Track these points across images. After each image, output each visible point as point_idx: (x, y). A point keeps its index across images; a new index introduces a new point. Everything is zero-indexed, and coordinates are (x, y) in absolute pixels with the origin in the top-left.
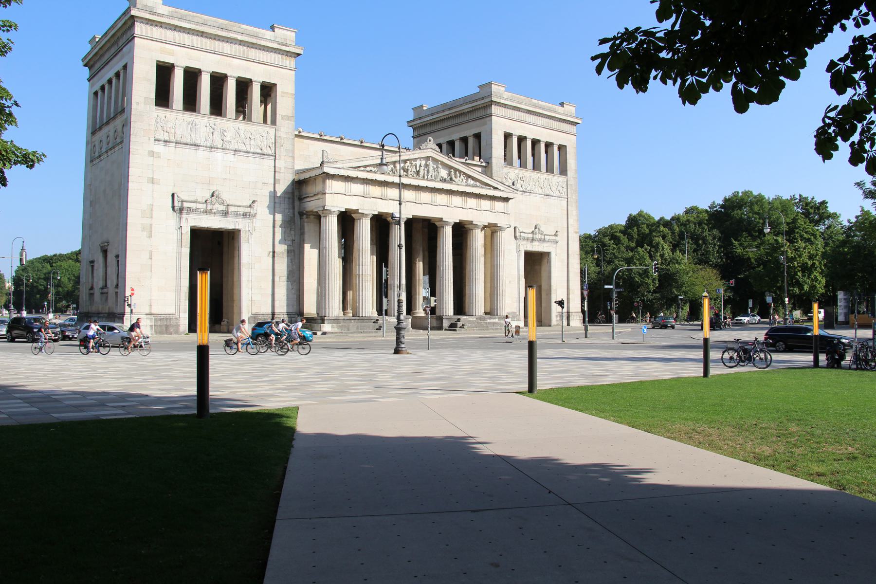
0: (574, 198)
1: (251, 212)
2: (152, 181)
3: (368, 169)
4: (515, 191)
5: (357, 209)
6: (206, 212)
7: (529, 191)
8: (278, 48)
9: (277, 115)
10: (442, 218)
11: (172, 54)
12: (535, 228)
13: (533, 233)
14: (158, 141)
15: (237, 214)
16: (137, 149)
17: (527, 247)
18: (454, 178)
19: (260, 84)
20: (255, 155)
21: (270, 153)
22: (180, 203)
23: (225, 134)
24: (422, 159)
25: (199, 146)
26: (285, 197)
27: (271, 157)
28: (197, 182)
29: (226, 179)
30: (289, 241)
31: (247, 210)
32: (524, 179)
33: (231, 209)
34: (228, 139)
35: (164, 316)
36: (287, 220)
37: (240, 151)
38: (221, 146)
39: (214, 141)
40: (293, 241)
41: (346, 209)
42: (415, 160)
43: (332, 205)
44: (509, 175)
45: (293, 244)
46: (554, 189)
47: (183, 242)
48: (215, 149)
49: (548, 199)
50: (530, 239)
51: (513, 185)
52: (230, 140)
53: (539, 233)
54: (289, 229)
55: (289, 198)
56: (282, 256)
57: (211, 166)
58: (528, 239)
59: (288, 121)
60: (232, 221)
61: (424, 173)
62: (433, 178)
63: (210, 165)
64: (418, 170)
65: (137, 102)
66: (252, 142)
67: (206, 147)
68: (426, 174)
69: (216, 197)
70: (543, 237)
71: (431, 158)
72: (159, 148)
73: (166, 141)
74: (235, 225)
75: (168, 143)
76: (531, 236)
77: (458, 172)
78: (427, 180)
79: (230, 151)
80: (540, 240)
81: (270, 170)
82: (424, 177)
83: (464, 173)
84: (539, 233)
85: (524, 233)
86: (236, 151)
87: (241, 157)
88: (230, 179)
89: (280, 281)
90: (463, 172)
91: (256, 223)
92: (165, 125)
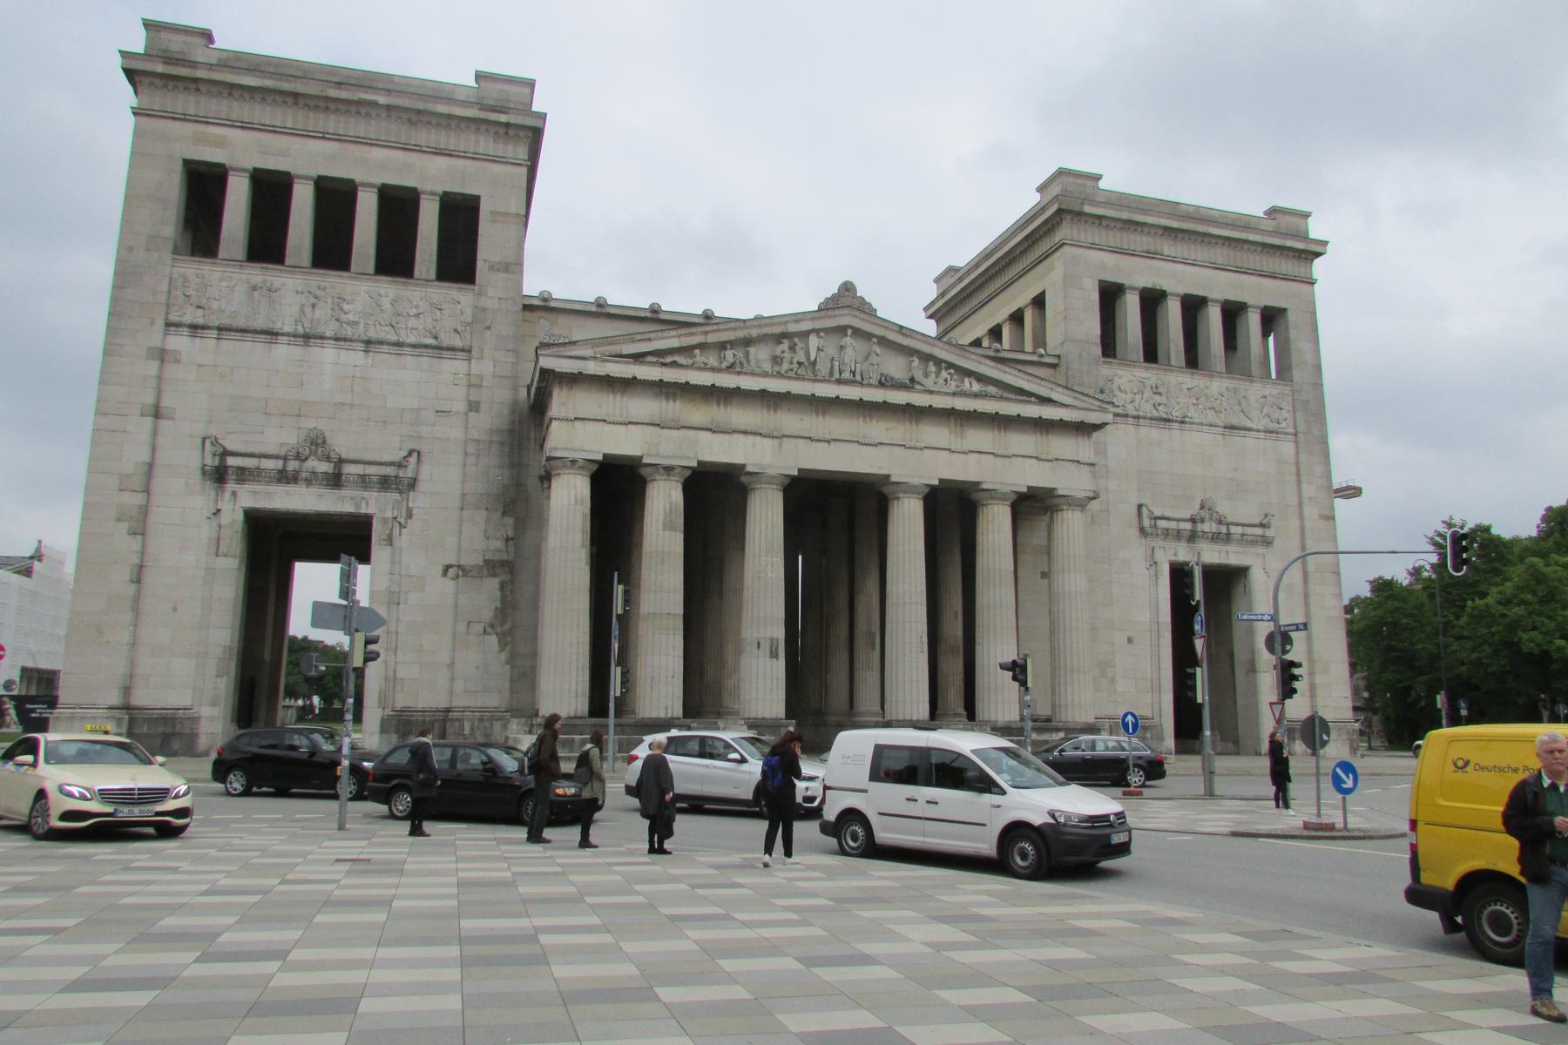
0: (1315, 432)
1: (401, 475)
2: (157, 413)
3: (669, 359)
4: (1104, 405)
5: (640, 454)
6: (285, 477)
7: (1180, 419)
8: (481, 117)
9: (480, 264)
10: (889, 476)
11: (221, 143)
12: (1202, 507)
13: (1193, 520)
14: (177, 325)
15: (364, 481)
16: (121, 346)
17: (1175, 554)
18: (919, 376)
19: (438, 198)
20: (421, 350)
21: (458, 343)
22: (217, 458)
23: (346, 307)
24: (822, 334)
26: (491, 442)
28: (268, 411)
29: (343, 404)
30: (497, 539)
31: (390, 471)
32: (1160, 390)
33: (349, 469)
34: (351, 317)
35: (160, 714)
36: (496, 492)
37: (381, 343)
38: (333, 333)
39: (314, 323)
40: (507, 540)
41: (605, 455)
42: (805, 335)
43: (569, 447)
44: (1117, 381)
45: (507, 547)
46: (1254, 414)
47: (221, 544)
49: (1237, 440)
50: (1186, 533)
51: (1102, 392)
52: (356, 320)
53: (1211, 519)
54: (499, 514)
55: (502, 444)
56: (476, 574)
57: (304, 378)
58: (1178, 535)
59: (505, 275)
60: (352, 498)
61: (832, 367)
62: (858, 378)
63: (302, 374)
64: (812, 359)
65: (129, 247)
66: (412, 323)
67: (295, 336)
68: (836, 369)
69: (311, 444)
70: (1224, 529)
71: (849, 332)
72: (179, 342)
73: (195, 328)
74: (358, 505)
76: (1188, 526)
77: (931, 364)
78: (839, 382)
80: (1215, 538)
82: (831, 374)
83: (950, 365)
84: (1211, 519)
85: (1168, 519)
86: (368, 342)
87: (383, 357)
88: (352, 405)
89: (468, 633)
90: (946, 362)
91: (414, 501)
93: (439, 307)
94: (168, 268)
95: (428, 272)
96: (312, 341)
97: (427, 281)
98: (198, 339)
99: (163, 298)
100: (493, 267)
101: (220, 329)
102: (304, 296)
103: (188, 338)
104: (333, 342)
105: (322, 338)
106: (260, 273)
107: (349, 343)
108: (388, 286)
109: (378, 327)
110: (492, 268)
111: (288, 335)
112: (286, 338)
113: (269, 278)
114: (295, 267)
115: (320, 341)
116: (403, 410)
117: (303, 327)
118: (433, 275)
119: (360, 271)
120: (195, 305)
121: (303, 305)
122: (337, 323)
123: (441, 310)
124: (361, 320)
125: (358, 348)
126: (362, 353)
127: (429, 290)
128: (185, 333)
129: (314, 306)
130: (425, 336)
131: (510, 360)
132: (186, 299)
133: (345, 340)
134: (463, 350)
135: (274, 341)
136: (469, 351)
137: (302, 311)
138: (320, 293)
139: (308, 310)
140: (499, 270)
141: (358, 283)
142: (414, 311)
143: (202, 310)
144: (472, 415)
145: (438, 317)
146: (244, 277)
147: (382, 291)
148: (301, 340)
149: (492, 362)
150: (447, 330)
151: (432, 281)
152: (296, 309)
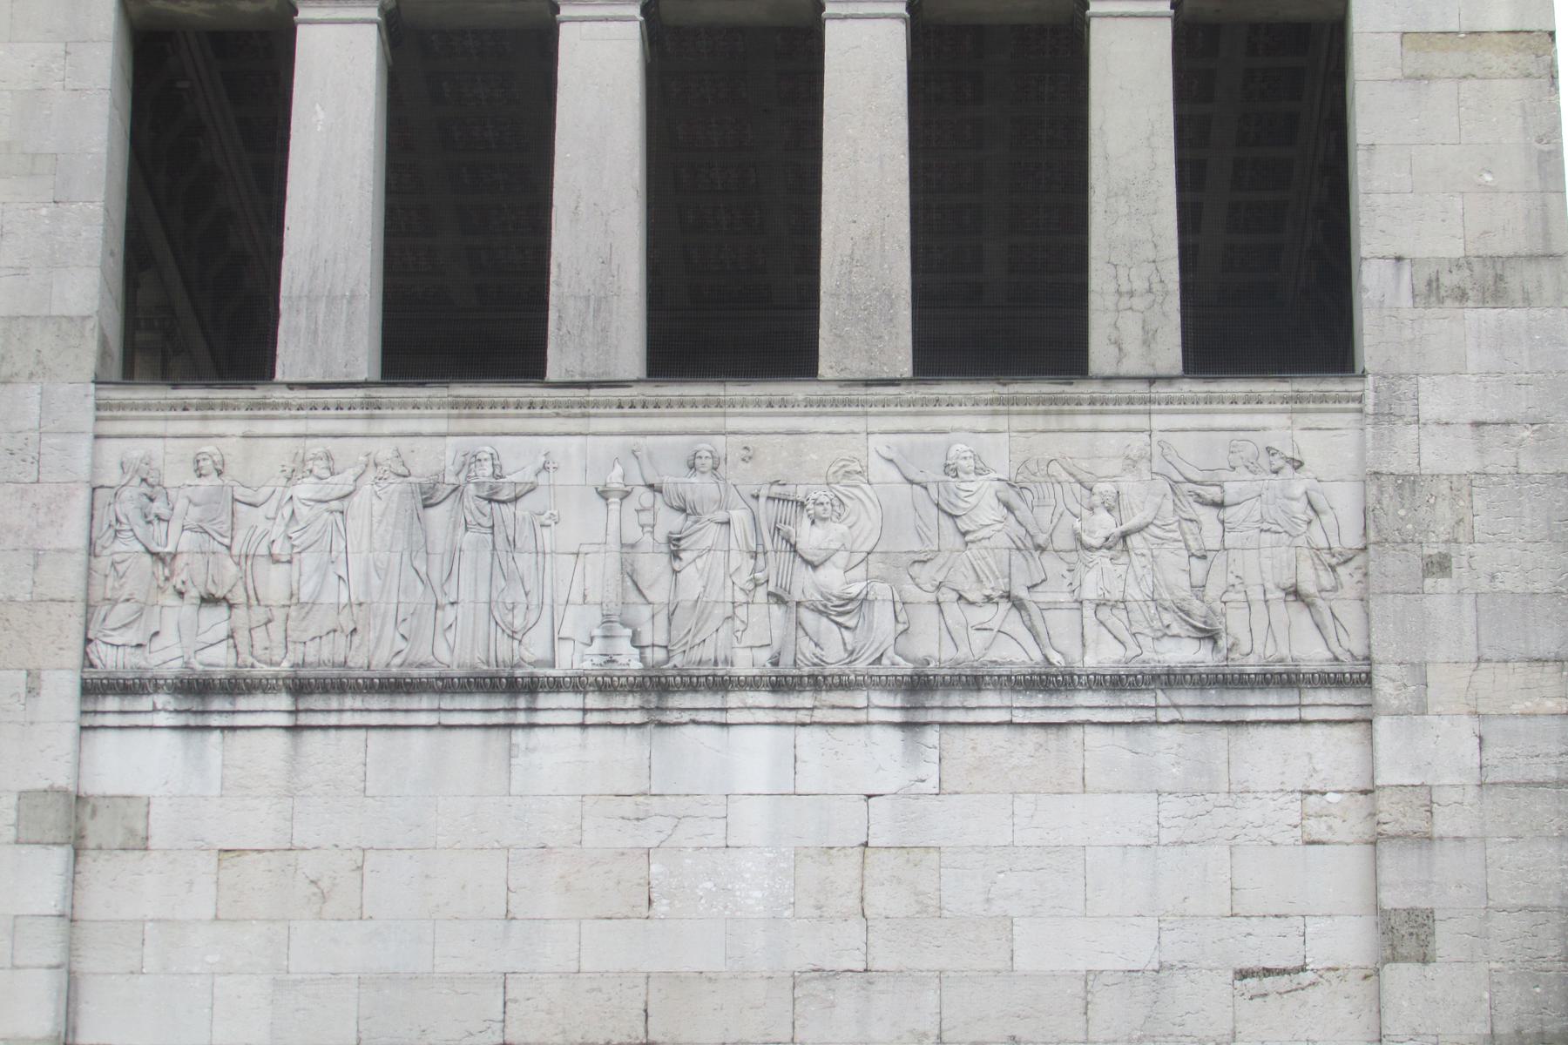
20: (1147, 699)
21: (1311, 652)
23: (810, 537)
25: (533, 687)
27: (1323, 696)
34: (833, 579)
37: (975, 682)
38: (764, 656)
39: (683, 621)
48: (702, 700)
52: (854, 590)
59: (1490, 314)
66: (1102, 575)
67: (606, 687)
75: (218, 703)
79: (859, 699)
81: (1316, 828)
86: (918, 685)
92: (187, 541)
93: (1212, 493)
94: (85, 443)
95: (1149, 338)
96: (686, 700)
97: (1152, 380)
98: (217, 735)
99: (67, 578)
100: (1433, 284)
101: (299, 687)
102: (631, 504)
103: (176, 737)
104: (765, 698)
105: (722, 685)
106: (442, 426)
107: (837, 697)
108: (983, 423)
109: (953, 611)
110: (1431, 292)
111: (578, 685)
112: (569, 700)
113: (484, 446)
114: (587, 385)
115: (714, 700)
116: (1089, 977)
117: (634, 640)
118: (1170, 354)
119: (858, 369)
120: (193, 594)
121: (629, 547)
122: (777, 611)
123: (1220, 505)
124: (881, 590)
125: (876, 715)
126: (896, 735)
127: (1158, 422)
128: (162, 719)
129: (674, 547)
130: (1164, 633)
131: (1550, 705)
132: (162, 571)
133: (817, 682)
134: (1334, 681)
135: (521, 718)
136: (1365, 681)
137: (630, 575)
138: (700, 487)
139: (653, 566)
140: (1462, 296)
141: (857, 424)
142: (1103, 525)
143: (223, 611)
144: (1400, 976)
145: (1212, 542)
146: (384, 450)
147: (960, 449)
148: (632, 701)
149: (1468, 726)
150: (1255, 594)
151: (1169, 379)
152: (600, 575)
